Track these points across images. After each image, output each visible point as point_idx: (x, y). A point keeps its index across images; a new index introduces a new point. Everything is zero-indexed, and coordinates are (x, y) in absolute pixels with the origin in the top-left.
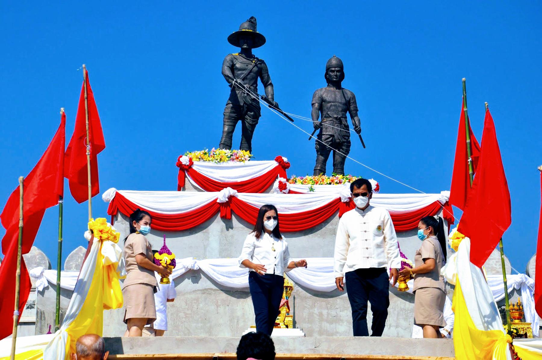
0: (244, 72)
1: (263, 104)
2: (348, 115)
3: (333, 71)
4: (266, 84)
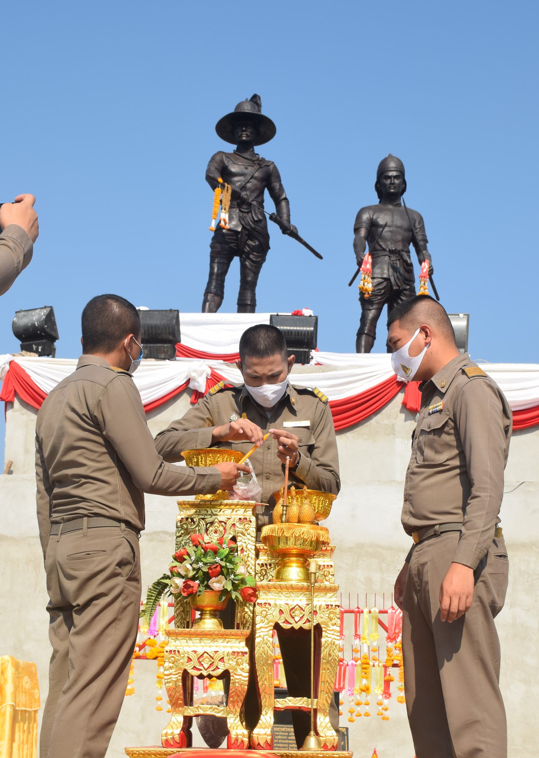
1: (273, 228)
2: (412, 248)
4: (278, 199)
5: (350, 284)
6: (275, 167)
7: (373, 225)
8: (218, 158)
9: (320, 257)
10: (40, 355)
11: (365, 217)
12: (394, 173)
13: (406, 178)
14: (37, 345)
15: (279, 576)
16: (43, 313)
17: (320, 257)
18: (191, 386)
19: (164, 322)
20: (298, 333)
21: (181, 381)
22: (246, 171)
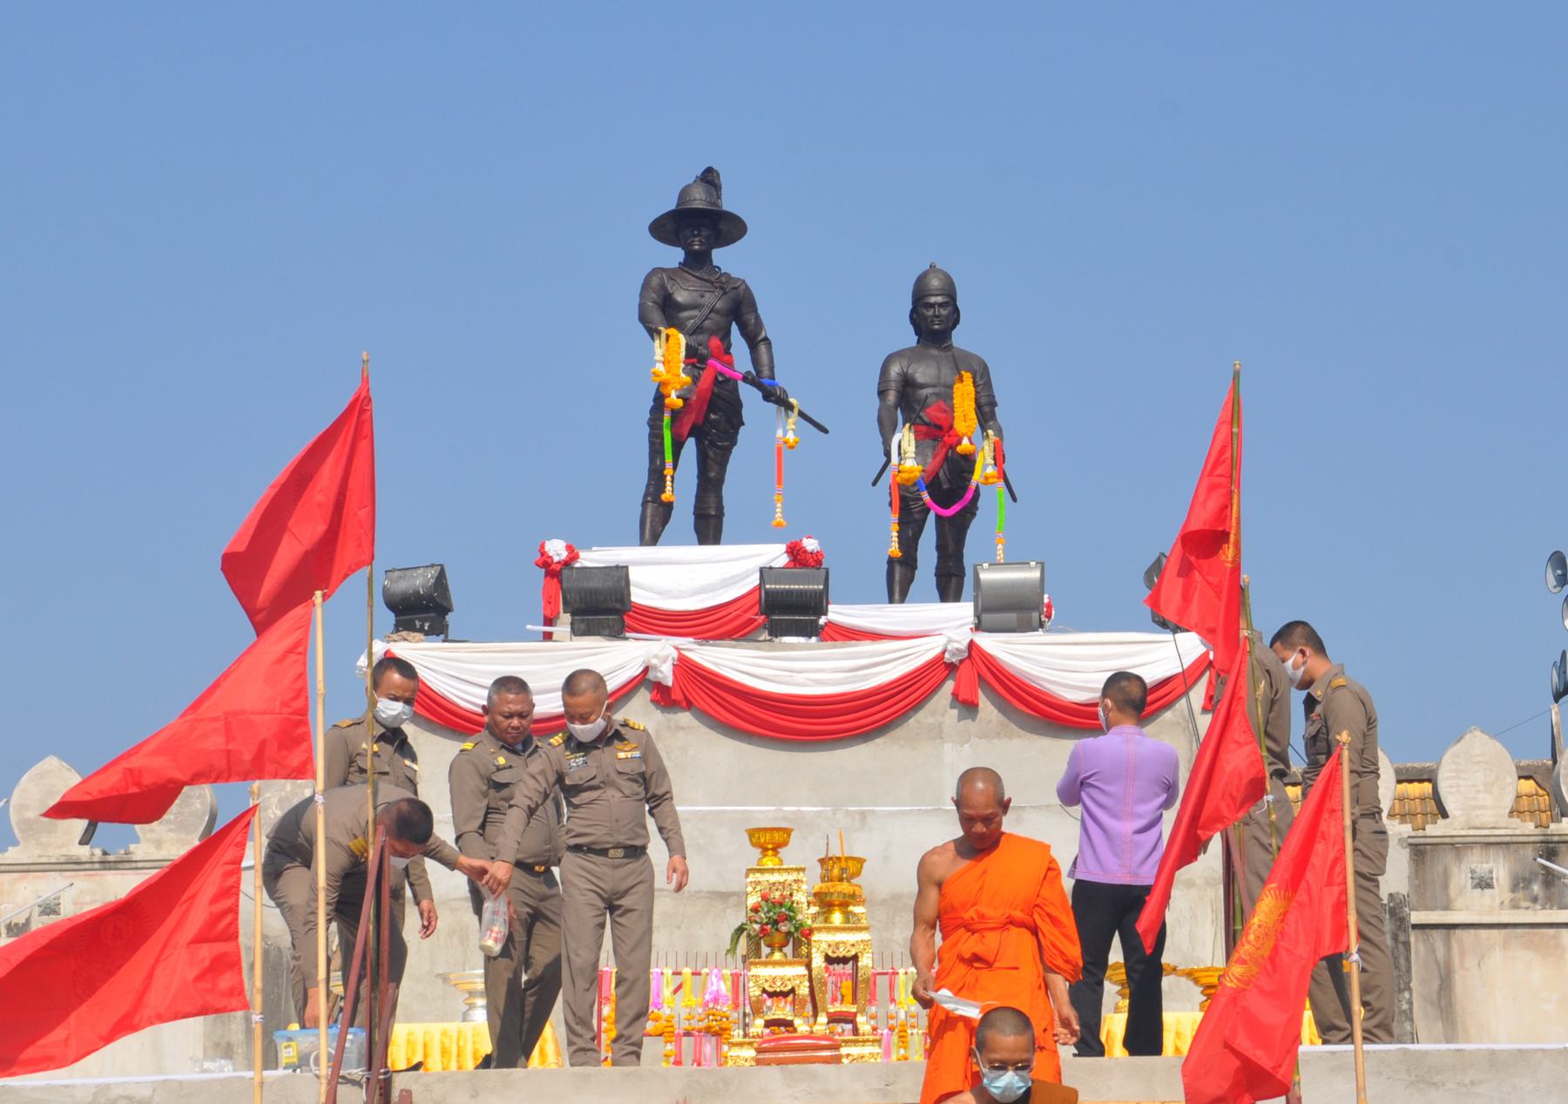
0: (695, 313)
1: (749, 395)
3: (932, 306)
4: (754, 339)
5: (874, 484)
6: (747, 289)
7: (908, 384)
8: (655, 281)
9: (825, 431)
10: (427, 634)
11: (895, 370)
12: (939, 299)
13: (958, 303)
14: (423, 621)
15: (826, 920)
16: (431, 574)
17: (825, 431)
18: (650, 676)
19: (609, 584)
20: (801, 593)
21: (634, 671)
22: (702, 301)
